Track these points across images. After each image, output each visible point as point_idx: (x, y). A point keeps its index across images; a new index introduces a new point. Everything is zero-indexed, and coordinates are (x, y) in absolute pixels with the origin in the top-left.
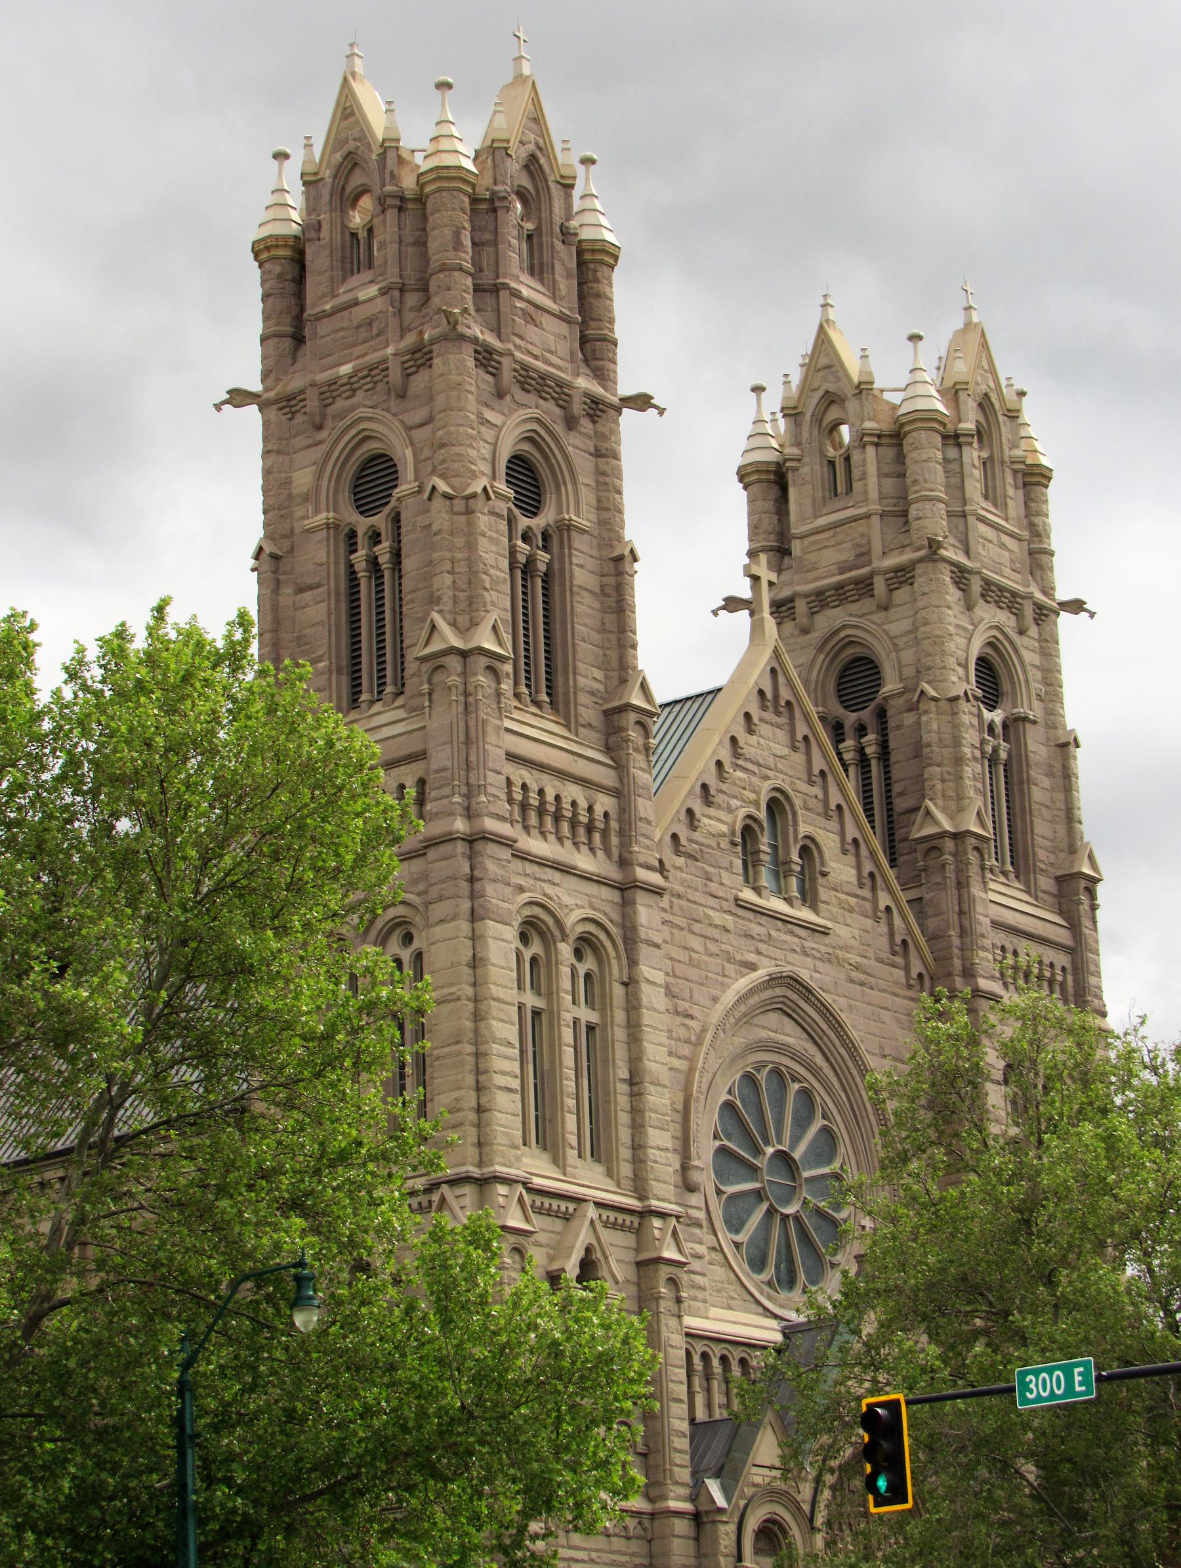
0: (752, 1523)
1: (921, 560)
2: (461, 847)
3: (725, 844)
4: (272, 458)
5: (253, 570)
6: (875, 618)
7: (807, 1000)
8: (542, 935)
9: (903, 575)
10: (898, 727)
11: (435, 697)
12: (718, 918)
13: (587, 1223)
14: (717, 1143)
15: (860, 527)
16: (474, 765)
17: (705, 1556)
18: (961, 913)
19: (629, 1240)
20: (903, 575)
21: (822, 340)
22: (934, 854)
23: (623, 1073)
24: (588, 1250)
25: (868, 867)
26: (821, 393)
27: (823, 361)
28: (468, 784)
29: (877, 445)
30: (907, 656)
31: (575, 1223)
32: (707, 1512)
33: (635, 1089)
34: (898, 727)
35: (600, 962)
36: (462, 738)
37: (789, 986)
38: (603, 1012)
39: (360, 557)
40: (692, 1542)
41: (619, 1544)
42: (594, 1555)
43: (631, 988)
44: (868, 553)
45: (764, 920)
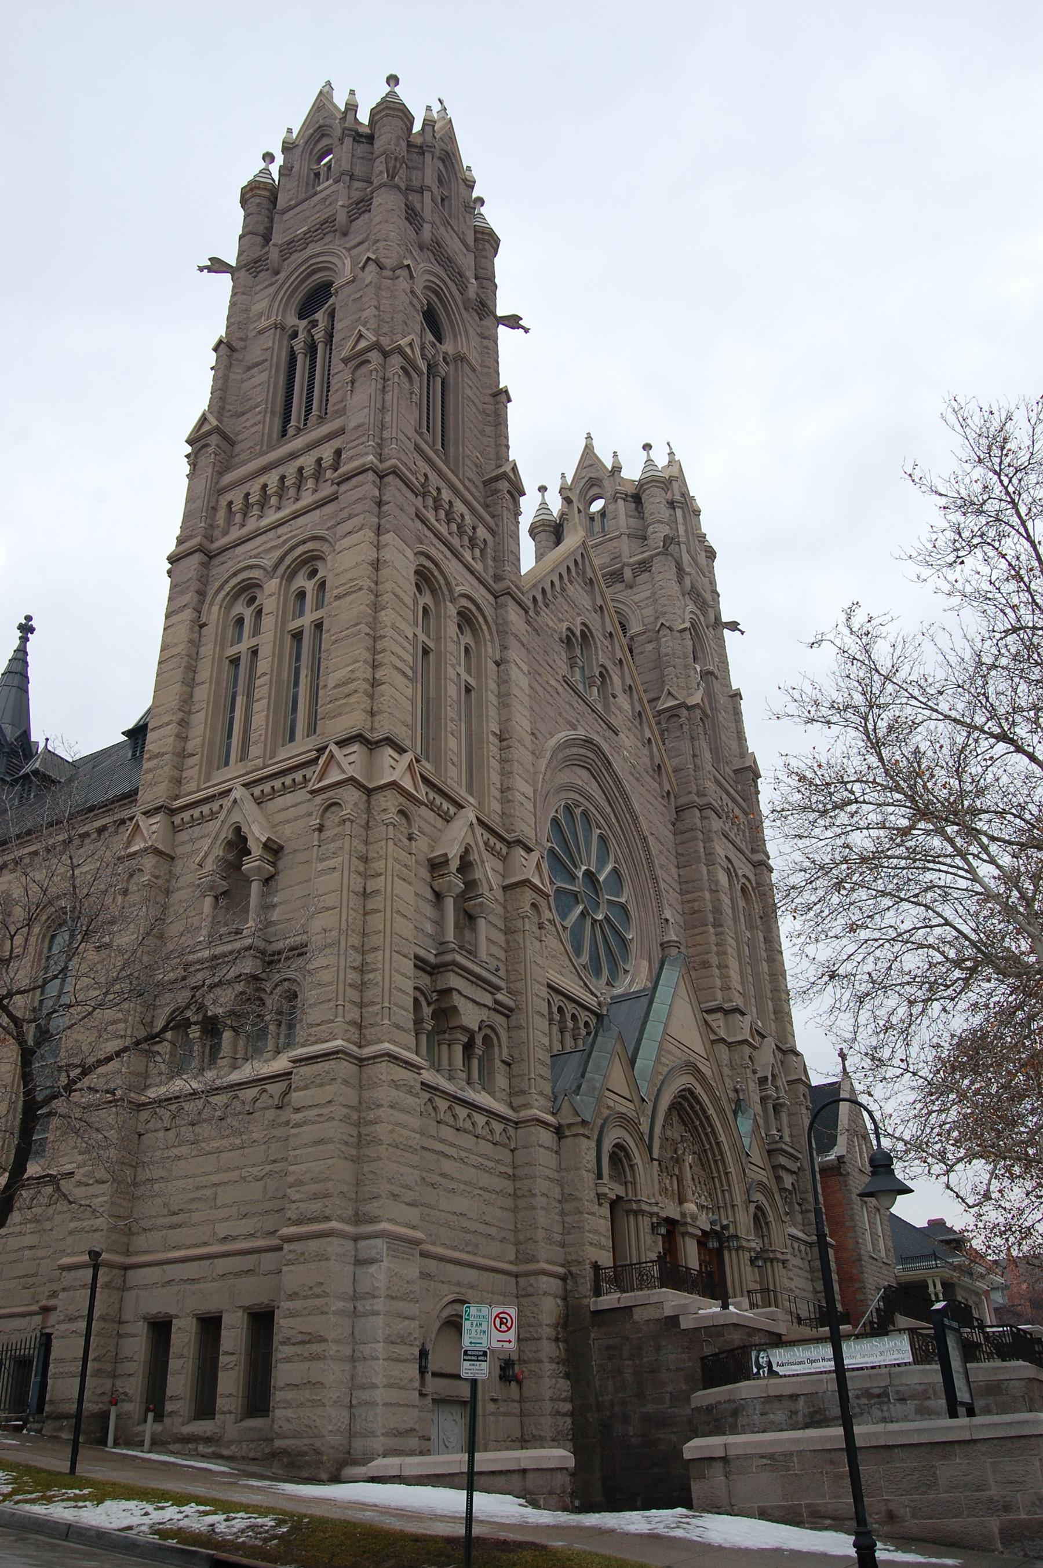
0: (607, 1147)
1: (658, 554)
2: (371, 476)
3: (556, 637)
4: (240, 298)
5: (212, 369)
6: (624, 593)
7: (607, 770)
8: (433, 591)
9: (644, 566)
10: (642, 653)
11: (356, 384)
12: (553, 682)
14: (550, 844)
15: (615, 543)
16: (388, 425)
19: (499, 865)
20: (644, 566)
21: (588, 449)
22: (674, 719)
27: (587, 463)
28: (381, 439)
29: (625, 500)
30: (648, 611)
32: (570, 1125)
33: (505, 743)
34: (642, 653)
36: (379, 405)
38: (478, 678)
39: (299, 344)
41: (486, 1148)
42: (463, 1154)
43: (502, 667)
44: (619, 556)
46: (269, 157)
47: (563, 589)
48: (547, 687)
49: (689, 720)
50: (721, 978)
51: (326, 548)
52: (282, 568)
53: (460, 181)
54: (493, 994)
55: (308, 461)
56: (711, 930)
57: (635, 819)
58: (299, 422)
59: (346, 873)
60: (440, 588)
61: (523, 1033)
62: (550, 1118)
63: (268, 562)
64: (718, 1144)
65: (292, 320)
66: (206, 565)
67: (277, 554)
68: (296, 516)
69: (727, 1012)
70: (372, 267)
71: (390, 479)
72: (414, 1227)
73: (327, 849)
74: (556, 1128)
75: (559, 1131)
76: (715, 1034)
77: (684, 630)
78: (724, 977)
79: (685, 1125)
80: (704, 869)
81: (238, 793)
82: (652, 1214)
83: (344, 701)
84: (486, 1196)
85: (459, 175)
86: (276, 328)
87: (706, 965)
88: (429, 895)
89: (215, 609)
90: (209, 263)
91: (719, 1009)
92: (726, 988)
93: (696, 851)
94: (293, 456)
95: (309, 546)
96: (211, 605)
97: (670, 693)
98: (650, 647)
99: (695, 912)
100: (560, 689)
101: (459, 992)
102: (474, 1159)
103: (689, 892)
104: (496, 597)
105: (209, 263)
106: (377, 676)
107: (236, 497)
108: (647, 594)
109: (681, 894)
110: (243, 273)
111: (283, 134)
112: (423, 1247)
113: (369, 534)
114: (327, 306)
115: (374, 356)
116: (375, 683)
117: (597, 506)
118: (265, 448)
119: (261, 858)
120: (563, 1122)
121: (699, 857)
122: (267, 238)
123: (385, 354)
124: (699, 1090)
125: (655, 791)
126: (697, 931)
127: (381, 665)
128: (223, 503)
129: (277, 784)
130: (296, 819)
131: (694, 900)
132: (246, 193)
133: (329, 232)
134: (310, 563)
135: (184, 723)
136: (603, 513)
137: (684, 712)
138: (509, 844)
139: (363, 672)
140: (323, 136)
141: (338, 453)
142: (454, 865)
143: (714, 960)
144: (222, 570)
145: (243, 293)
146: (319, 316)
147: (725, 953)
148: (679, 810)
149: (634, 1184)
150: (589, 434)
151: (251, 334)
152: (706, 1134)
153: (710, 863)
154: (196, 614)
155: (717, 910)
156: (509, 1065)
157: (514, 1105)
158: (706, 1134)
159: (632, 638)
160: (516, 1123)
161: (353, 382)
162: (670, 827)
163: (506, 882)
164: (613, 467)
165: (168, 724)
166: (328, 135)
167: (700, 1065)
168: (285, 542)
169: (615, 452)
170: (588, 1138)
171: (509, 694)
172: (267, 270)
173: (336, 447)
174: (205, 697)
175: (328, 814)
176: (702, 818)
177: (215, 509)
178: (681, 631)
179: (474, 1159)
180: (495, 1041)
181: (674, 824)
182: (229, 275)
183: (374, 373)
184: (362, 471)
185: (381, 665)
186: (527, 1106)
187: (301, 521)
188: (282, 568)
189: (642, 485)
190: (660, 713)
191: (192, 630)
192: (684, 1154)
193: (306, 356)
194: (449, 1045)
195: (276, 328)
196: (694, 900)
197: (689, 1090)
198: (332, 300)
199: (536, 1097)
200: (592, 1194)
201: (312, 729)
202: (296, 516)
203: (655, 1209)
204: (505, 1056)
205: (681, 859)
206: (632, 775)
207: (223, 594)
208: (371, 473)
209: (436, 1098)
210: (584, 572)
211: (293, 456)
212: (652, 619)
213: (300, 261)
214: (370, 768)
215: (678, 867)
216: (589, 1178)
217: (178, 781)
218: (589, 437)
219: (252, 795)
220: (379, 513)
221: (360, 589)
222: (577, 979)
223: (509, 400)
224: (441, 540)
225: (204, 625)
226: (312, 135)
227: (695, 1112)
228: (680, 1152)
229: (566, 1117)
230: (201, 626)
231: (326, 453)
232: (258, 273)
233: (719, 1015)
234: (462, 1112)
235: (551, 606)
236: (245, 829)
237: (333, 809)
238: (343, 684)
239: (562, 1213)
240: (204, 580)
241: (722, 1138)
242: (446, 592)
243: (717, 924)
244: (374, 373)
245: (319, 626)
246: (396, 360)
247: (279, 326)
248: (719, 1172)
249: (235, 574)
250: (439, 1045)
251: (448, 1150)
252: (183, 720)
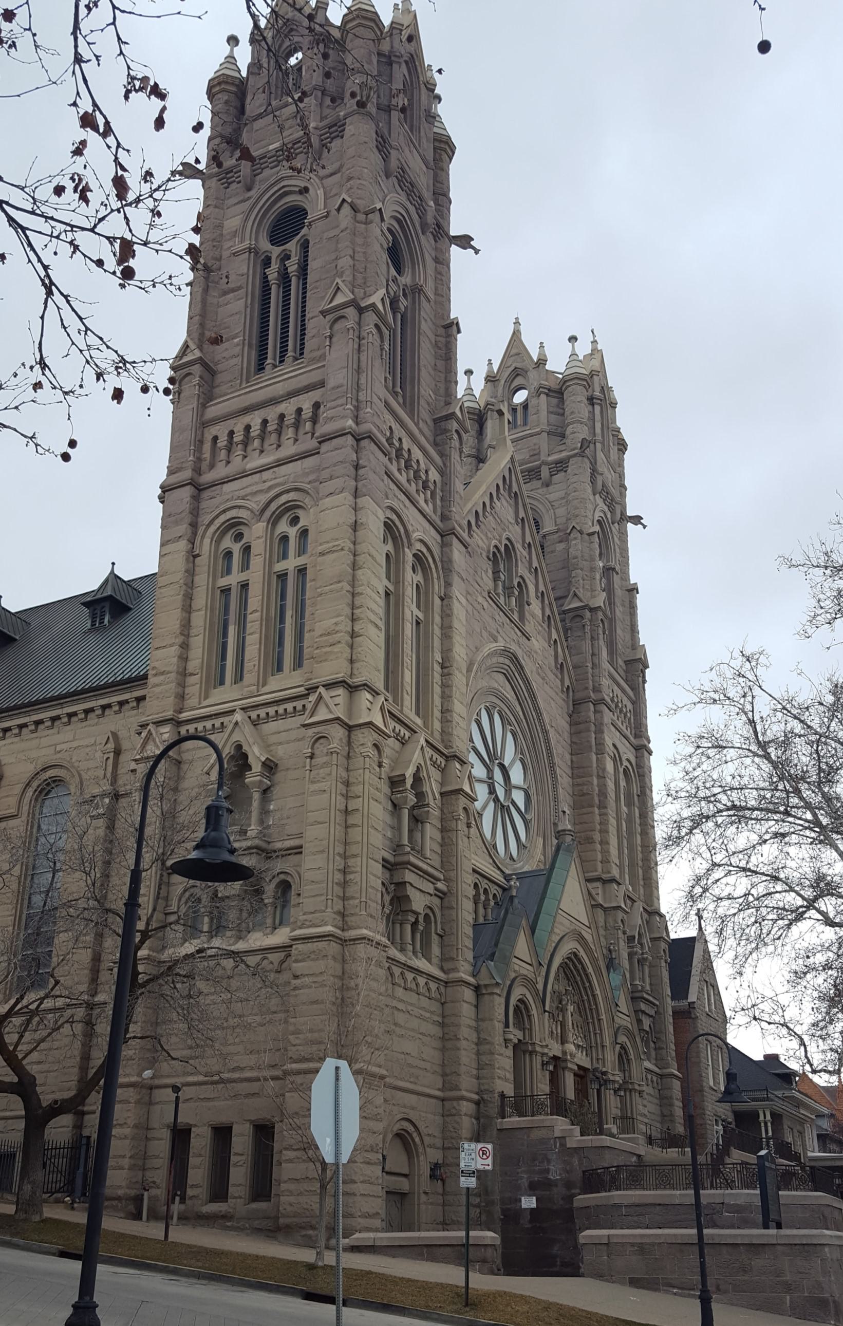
0: (513, 1001)
1: (575, 456)
2: (350, 440)
6: (540, 491)
7: (520, 674)
9: (561, 466)
10: (552, 552)
11: (334, 339)
12: (480, 599)
13: (420, 747)
15: (534, 439)
16: (363, 387)
17: (483, 1020)
18: (593, 655)
20: (561, 466)
22: (578, 619)
23: (438, 657)
24: (418, 769)
25: (548, 612)
26: (512, 368)
28: (357, 400)
29: (547, 395)
30: (561, 512)
31: (409, 747)
32: (486, 986)
33: (446, 671)
34: (552, 552)
35: (426, 580)
36: (355, 367)
37: (511, 660)
38: (426, 612)
40: (473, 1009)
41: (425, 1002)
42: (410, 1008)
43: (445, 602)
44: (539, 454)
45: (501, 613)
46: (233, 40)
47: (492, 507)
48: (475, 605)
49: (591, 621)
50: (601, 852)
51: (307, 500)
52: (268, 513)
54: (433, 884)
55: (288, 408)
56: (597, 811)
57: (539, 714)
58: (275, 359)
59: (333, 796)
60: (400, 536)
61: (454, 913)
62: (471, 980)
63: (256, 504)
64: (594, 996)
65: (265, 245)
66: (196, 498)
67: (263, 498)
68: (280, 463)
69: (605, 882)
70: (346, 209)
71: (365, 443)
72: (380, 1066)
73: (318, 774)
74: (476, 987)
75: (477, 989)
76: (594, 899)
77: (593, 533)
78: (606, 853)
79: (568, 979)
80: (594, 757)
82: (543, 1054)
83: (328, 649)
84: (424, 1039)
86: (250, 253)
87: (590, 840)
88: (390, 807)
89: (207, 541)
91: (598, 879)
92: (606, 861)
93: (588, 741)
94: (274, 401)
95: (292, 496)
96: (203, 537)
97: (575, 595)
98: (561, 546)
99: (583, 795)
100: (485, 604)
101: (411, 884)
102: (417, 1011)
103: (580, 777)
104: (442, 536)
106: (356, 629)
108: (562, 494)
109: (572, 778)
110: (213, 182)
112: (387, 1080)
113: (346, 498)
114: (298, 237)
115: (351, 312)
116: (353, 635)
117: (520, 397)
119: (262, 775)
120: (482, 983)
121: (591, 747)
123: (361, 310)
124: (582, 953)
125: (557, 687)
126: (584, 810)
127: (359, 619)
128: (208, 437)
129: (271, 710)
130: (288, 742)
131: (583, 784)
132: (214, 86)
134: (291, 511)
135: (185, 646)
136: (525, 405)
137: (588, 614)
138: (447, 758)
139: (346, 625)
141: (317, 406)
142: (409, 782)
143: (597, 837)
144: (212, 503)
145: (216, 207)
146: (292, 246)
147: (606, 814)
148: (577, 703)
149: (531, 1030)
150: (517, 318)
151: (226, 254)
152: (585, 988)
153: (600, 751)
154: (190, 546)
155: (603, 794)
156: (441, 936)
157: (445, 968)
158: (585, 988)
159: (544, 537)
160: (446, 983)
161: (331, 337)
162: (568, 719)
163: (444, 790)
164: (539, 360)
165: (171, 646)
167: (583, 933)
168: (270, 488)
169: (541, 343)
170: (500, 995)
171: (451, 627)
172: (239, 182)
173: (314, 400)
174: (202, 623)
175: (317, 745)
176: (595, 712)
177: (201, 442)
178: (590, 534)
179: (417, 1011)
180: (433, 918)
181: (570, 716)
183: (351, 331)
184: (341, 434)
185: (359, 619)
186: (455, 970)
187: (284, 469)
188: (268, 513)
189: (565, 382)
190: (564, 612)
191: (187, 560)
192: (567, 1004)
193: (279, 286)
194: (401, 924)
196: (583, 784)
197: (574, 953)
198: (303, 232)
199: (463, 963)
200: (502, 1039)
201: (298, 663)
202: (280, 463)
203: (546, 1051)
204: (439, 931)
205: (574, 746)
206: (539, 674)
208: (349, 436)
209: (393, 967)
210: (510, 487)
211: (274, 401)
212: (564, 520)
213: (272, 181)
214: (350, 710)
215: (571, 754)
216: (499, 1026)
217: (181, 697)
218: (517, 323)
219: (250, 717)
220: (356, 475)
221: (342, 549)
222: (488, 858)
223: (459, 331)
224: (401, 490)
225: (198, 555)
227: (578, 971)
228: (564, 1003)
229: (484, 980)
230: (195, 557)
231: (306, 403)
232: (229, 184)
233: (598, 884)
234: (410, 976)
235: (482, 526)
236: (245, 748)
237: (322, 741)
238: (329, 634)
239: (478, 1053)
240: (195, 512)
241: (598, 992)
242: (405, 540)
243: (603, 806)
244: (351, 331)
245: (302, 571)
246: (370, 319)
247: (253, 251)
248: (593, 1018)
249: (224, 511)
250: (393, 923)
251: (401, 1006)
252: (184, 643)
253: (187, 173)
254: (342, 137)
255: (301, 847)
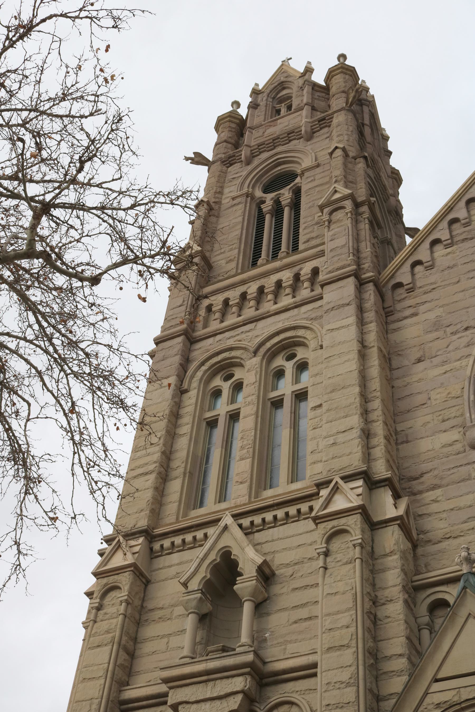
51: (308, 334)
53: (380, 137)
65: (259, 193)
81: (228, 520)
85: (379, 133)
86: (247, 197)
90: (193, 156)
96: (192, 377)
105: (193, 156)
107: (217, 300)
111: (252, 86)
118: (239, 271)
122: (237, 146)
133: (295, 139)
140: (284, 88)
166: (288, 88)
182: (206, 168)
195: (247, 197)
207: (204, 368)
225: (186, 391)
226: (276, 86)
253: (196, 159)
254: (329, 126)
255: (315, 666)
